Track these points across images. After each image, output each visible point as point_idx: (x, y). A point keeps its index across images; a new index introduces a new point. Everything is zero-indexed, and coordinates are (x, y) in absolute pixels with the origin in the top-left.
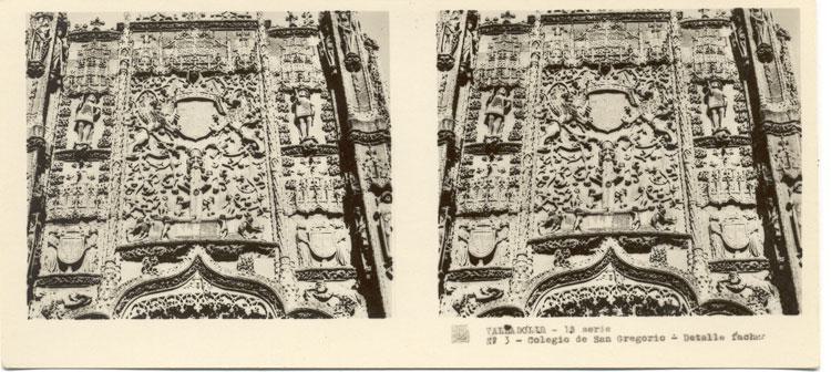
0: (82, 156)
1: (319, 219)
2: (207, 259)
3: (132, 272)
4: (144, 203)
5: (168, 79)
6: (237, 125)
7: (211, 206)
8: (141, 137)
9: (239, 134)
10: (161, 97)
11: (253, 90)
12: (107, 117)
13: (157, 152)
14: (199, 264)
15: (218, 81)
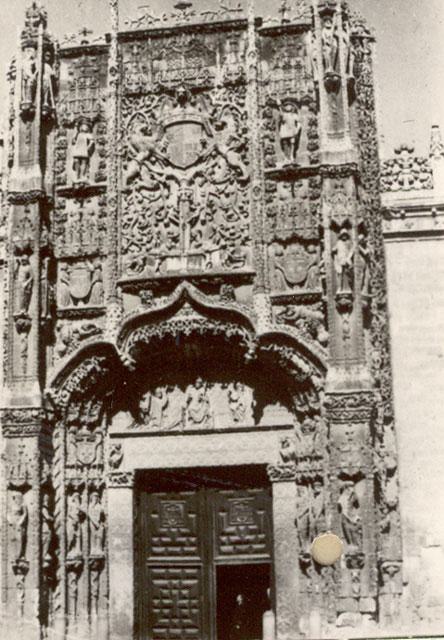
2: (192, 289)
3: (134, 306)
4: (139, 237)
5: (157, 98)
6: (224, 149)
8: (133, 167)
9: (225, 157)
10: (148, 120)
13: (147, 181)
14: (185, 297)
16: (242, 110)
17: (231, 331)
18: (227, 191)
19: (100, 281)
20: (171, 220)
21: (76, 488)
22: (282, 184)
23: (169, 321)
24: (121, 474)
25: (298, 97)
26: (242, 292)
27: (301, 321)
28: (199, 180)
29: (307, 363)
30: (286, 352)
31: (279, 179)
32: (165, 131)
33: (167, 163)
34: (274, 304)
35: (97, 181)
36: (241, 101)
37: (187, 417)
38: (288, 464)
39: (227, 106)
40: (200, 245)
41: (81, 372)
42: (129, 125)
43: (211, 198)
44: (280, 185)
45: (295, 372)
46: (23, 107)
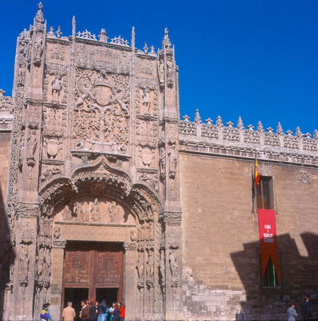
0: (55, 107)
1: (147, 150)
2: (106, 161)
3: (78, 163)
4: (81, 132)
5: (91, 72)
6: (120, 101)
7: (107, 137)
8: (80, 100)
9: (120, 105)
10: (88, 81)
11: (127, 85)
12: (65, 88)
13: (87, 109)
15: (113, 77)
16: (128, 87)
17: (120, 179)
18: (120, 120)
19: (61, 149)
20: (96, 127)
21: (43, 246)
22: (142, 121)
23: (93, 172)
24: (59, 242)
25: (151, 87)
26: (125, 164)
27: (148, 181)
28: (108, 112)
29: (150, 198)
30: (142, 192)
31: (141, 119)
32: (95, 87)
33: (96, 102)
34: (138, 171)
35: (63, 103)
36: (127, 83)
37: (90, 218)
38: (133, 242)
39: (122, 83)
40: (108, 141)
41: (52, 190)
42: (79, 81)
43: (114, 121)
44: (141, 122)
45: (144, 202)
46: (36, 60)
